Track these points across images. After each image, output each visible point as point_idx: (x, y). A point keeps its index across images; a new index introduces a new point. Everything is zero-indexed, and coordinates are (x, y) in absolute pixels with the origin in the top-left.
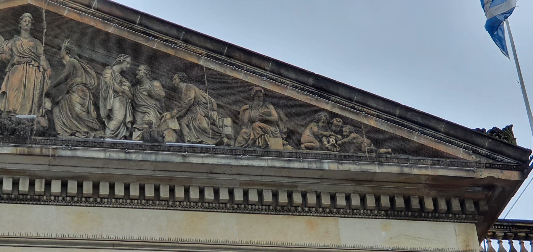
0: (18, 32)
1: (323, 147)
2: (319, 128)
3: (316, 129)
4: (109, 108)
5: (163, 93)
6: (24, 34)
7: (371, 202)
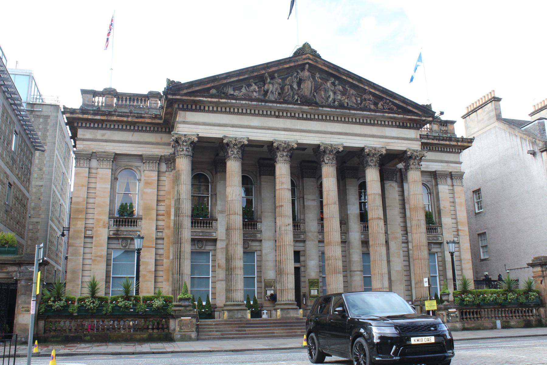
1: (384, 109)
2: (383, 103)
3: (382, 103)
4: (329, 94)
5: (342, 90)
6: (306, 70)
7: (394, 124)
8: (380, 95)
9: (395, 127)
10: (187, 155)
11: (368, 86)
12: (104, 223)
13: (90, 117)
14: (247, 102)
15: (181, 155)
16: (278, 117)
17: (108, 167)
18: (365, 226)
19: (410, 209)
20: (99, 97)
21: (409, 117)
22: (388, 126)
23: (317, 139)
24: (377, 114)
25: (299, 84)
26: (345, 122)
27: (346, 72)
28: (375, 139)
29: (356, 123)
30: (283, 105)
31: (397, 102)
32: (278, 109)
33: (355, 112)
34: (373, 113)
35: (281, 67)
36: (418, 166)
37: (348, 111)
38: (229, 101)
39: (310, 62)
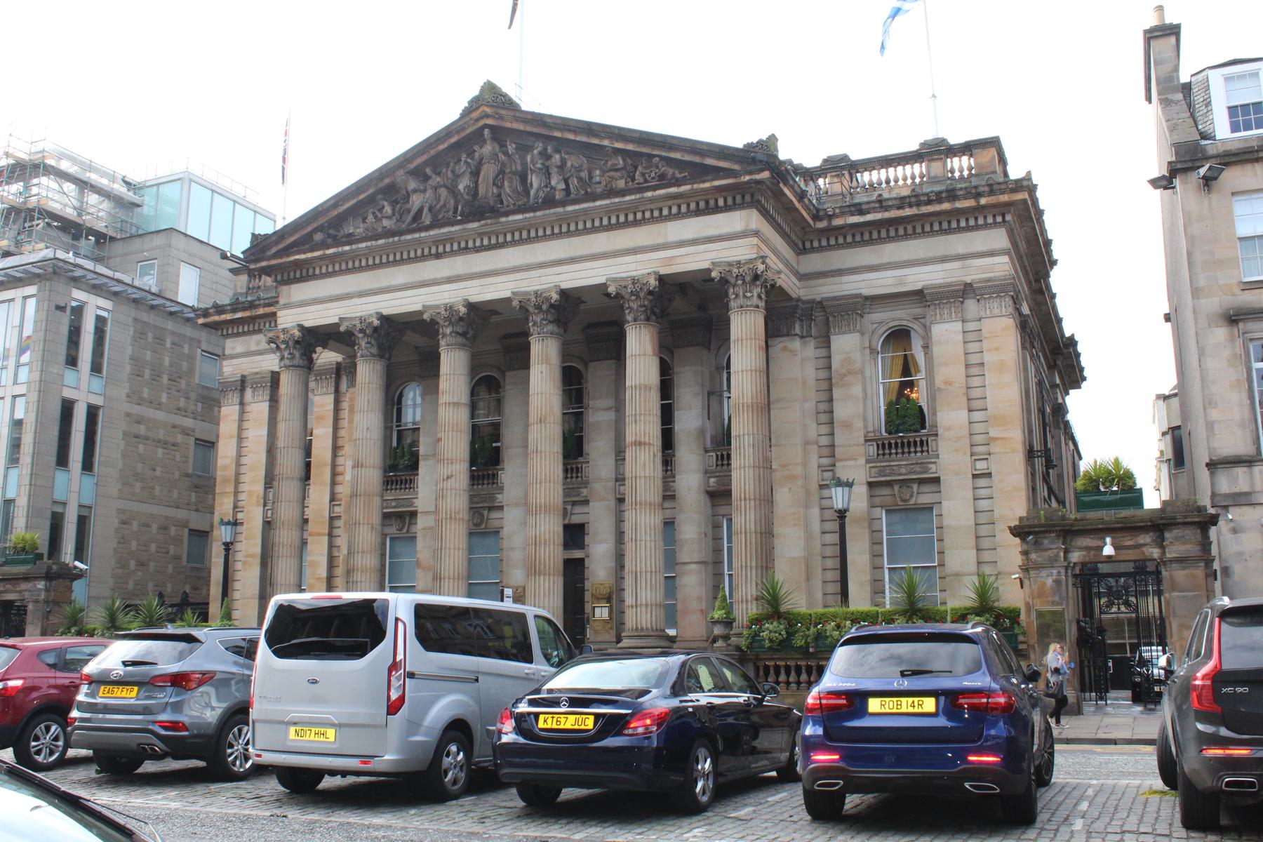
0: (485, 141)
1: (646, 181)
6: (488, 142)
8: (637, 149)
10: (290, 366)
11: (609, 138)
12: (258, 497)
13: (228, 317)
14: (369, 244)
16: (438, 256)
17: (260, 398)
18: (722, 455)
20: (887, 168)
21: (707, 185)
22: (671, 217)
24: (628, 198)
25: (476, 174)
26: (569, 234)
27: (559, 121)
28: (639, 257)
29: (594, 230)
30: (432, 233)
31: (676, 155)
32: (433, 242)
33: (577, 207)
34: (617, 200)
35: (433, 152)
36: (745, 300)
37: (560, 210)
38: (340, 249)
39: (489, 121)
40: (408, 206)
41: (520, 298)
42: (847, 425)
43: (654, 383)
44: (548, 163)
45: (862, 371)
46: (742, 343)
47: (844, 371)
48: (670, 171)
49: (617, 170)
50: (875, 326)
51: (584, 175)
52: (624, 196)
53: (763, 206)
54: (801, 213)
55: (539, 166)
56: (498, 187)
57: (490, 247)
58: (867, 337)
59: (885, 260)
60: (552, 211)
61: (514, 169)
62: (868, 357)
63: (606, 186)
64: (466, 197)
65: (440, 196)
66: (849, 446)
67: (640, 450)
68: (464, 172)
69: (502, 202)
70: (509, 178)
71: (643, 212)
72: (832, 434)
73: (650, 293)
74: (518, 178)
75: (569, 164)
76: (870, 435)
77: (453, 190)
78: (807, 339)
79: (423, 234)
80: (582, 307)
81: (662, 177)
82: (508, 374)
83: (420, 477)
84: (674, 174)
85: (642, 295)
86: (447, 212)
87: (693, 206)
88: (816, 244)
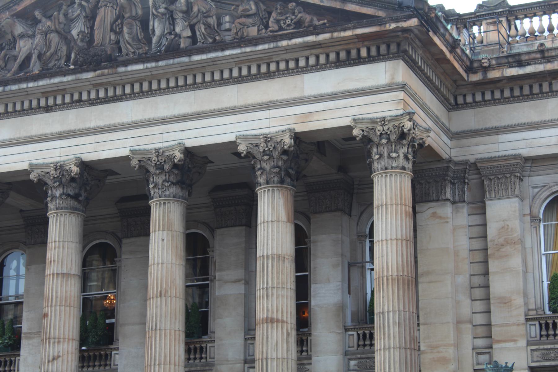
1: (281, 29)
9: (331, 68)
15: (392, 168)
16: (48, 109)
18: (364, 335)
19: (392, 279)
20: (550, 15)
21: (349, 33)
22: (308, 69)
23: (231, 128)
24: (260, 47)
25: (91, 18)
26: (195, 86)
29: (223, 82)
30: (41, 83)
32: (43, 93)
33: (204, 57)
34: (248, 49)
36: (390, 161)
37: (185, 59)
40: (15, 53)
41: (140, 157)
42: (505, 302)
43: (289, 253)
44: (172, 8)
45: (522, 241)
46: (386, 208)
47: (501, 240)
48: (307, 18)
49: (248, 16)
50: (536, 190)
51: (212, 21)
52: (256, 45)
53: (410, 57)
54: (453, 65)
55: (162, 10)
56: (116, 33)
57: (107, 100)
58: (527, 202)
59: (547, 117)
60: (177, 60)
61: (134, 14)
62: (528, 225)
63: (236, 33)
64: (80, 44)
65: (50, 42)
66: (507, 325)
67: (272, 328)
68: (78, 15)
69: (120, 50)
70: (128, 24)
71: (278, 63)
72: (489, 312)
73: (285, 152)
74: (138, 24)
75: (195, 9)
76: (531, 313)
77: (65, 37)
78: (460, 205)
79: (31, 85)
80: (209, 167)
81: (299, 24)
82: (124, 241)
83: (22, 358)
84: (312, 20)
85: (275, 154)
86: (58, 60)
87: (332, 56)
88: (469, 99)
